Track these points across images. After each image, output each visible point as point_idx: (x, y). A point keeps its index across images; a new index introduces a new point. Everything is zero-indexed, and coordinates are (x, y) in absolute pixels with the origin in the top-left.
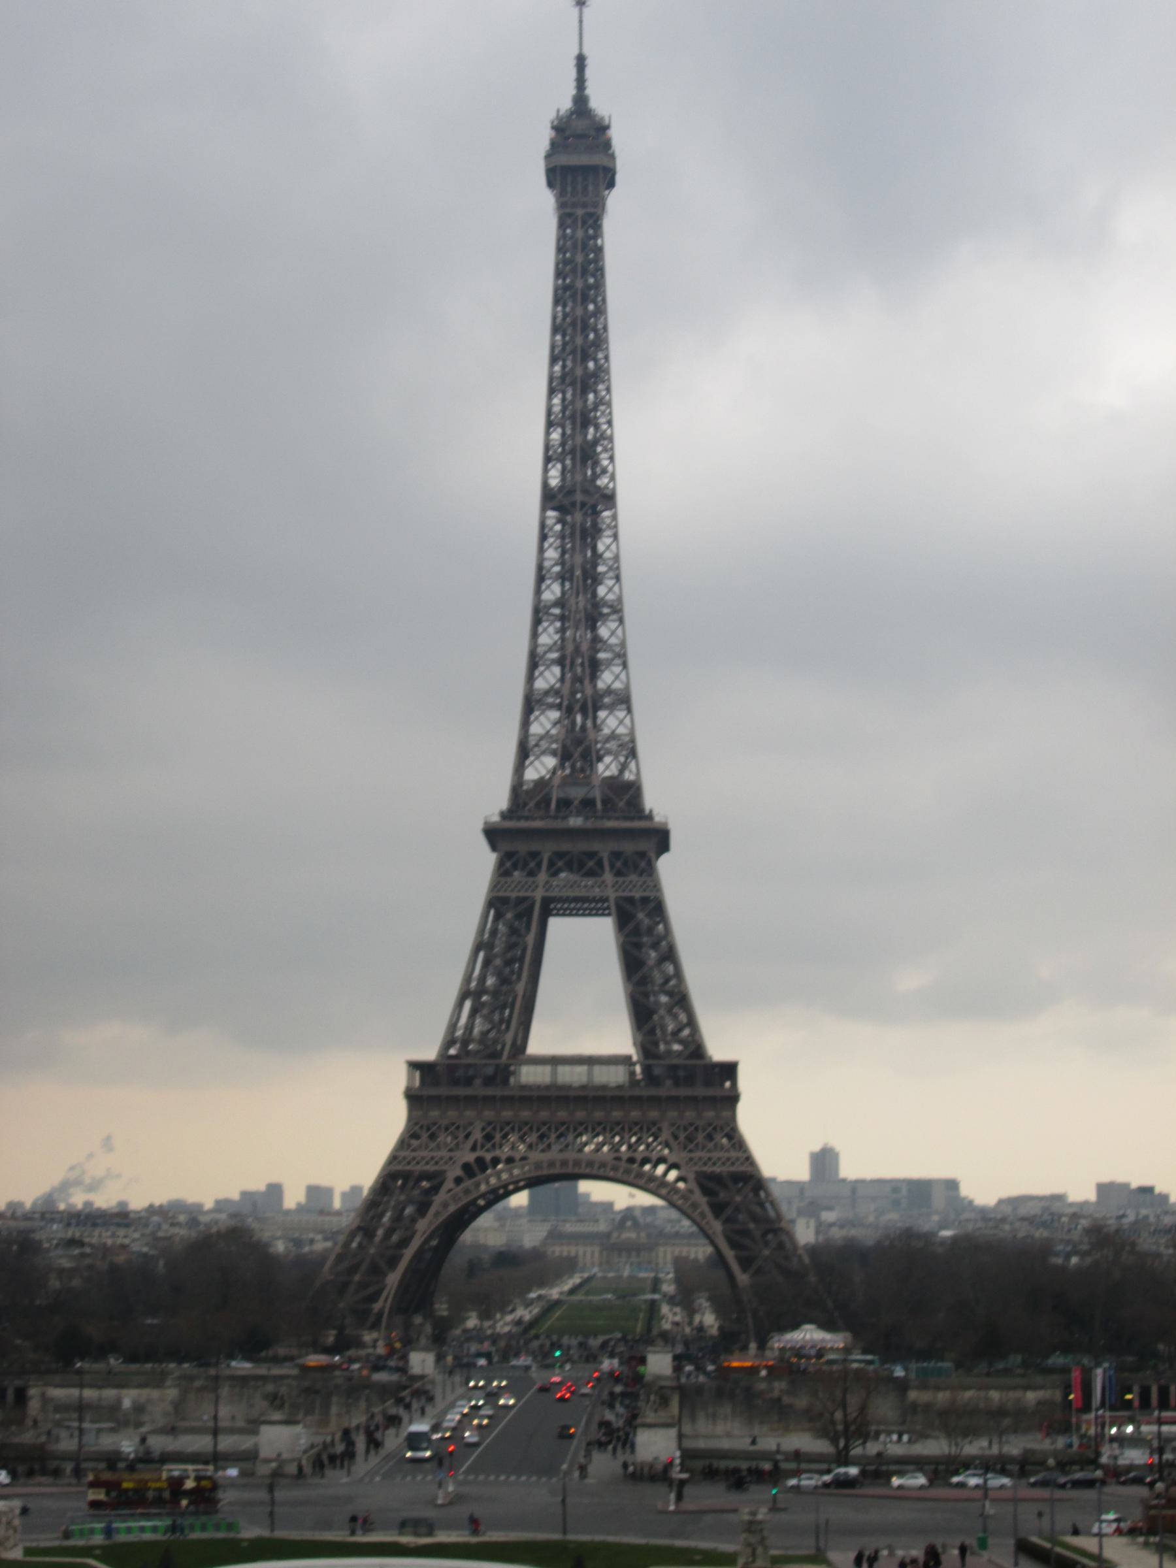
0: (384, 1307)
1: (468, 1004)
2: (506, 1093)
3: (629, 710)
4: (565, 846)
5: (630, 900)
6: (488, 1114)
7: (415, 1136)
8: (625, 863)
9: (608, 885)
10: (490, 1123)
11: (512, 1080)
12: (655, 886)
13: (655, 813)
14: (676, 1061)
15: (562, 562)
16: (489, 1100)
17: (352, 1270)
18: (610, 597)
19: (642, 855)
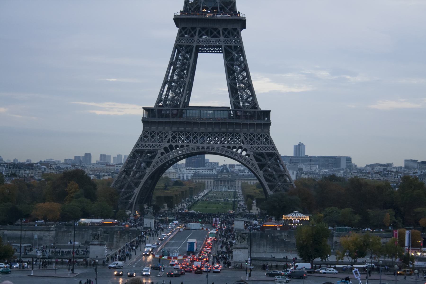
0: (133, 201)
1: (167, 86)
2: (180, 120)
5: (230, 47)
6: (174, 129)
7: (146, 137)
9: (221, 41)
10: (174, 132)
11: (184, 115)
12: (240, 42)
13: (240, 13)
14: (246, 110)
16: (174, 123)
17: (121, 187)
19: (235, 30)
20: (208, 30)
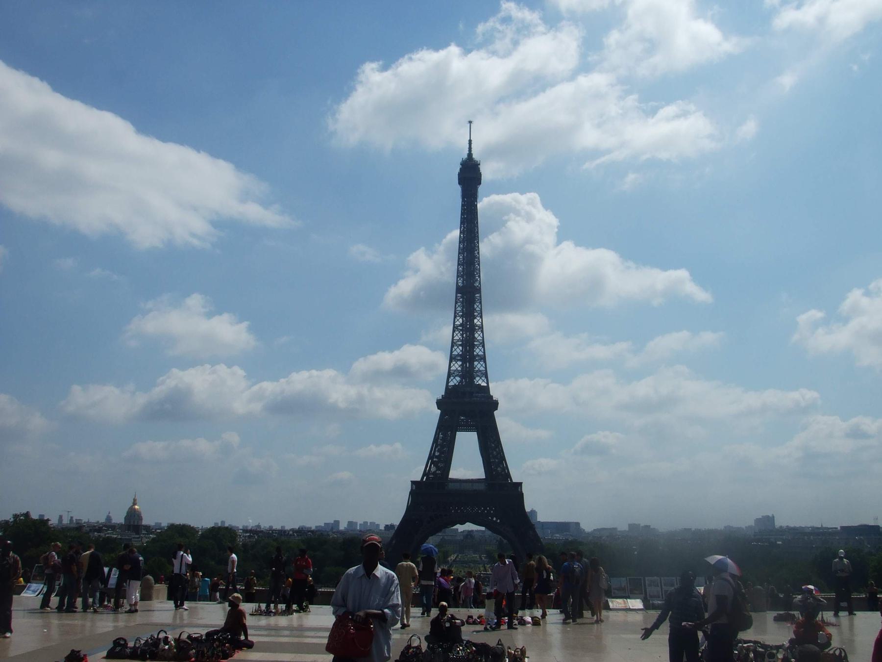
3: (485, 362)
15: (462, 311)
18: (479, 323)
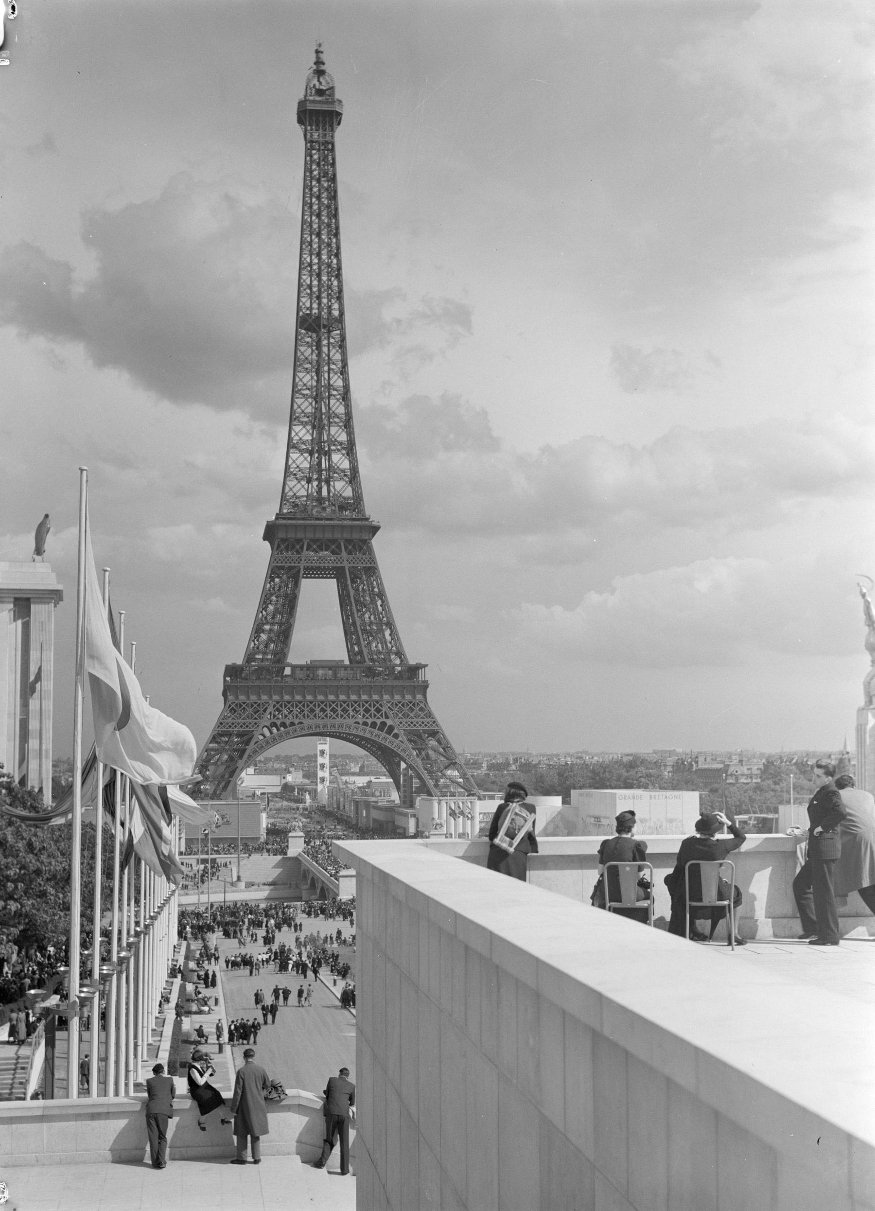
4: (319, 535)
8: (354, 547)
9: (346, 560)
10: (278, 703)
20: (322, 544)
